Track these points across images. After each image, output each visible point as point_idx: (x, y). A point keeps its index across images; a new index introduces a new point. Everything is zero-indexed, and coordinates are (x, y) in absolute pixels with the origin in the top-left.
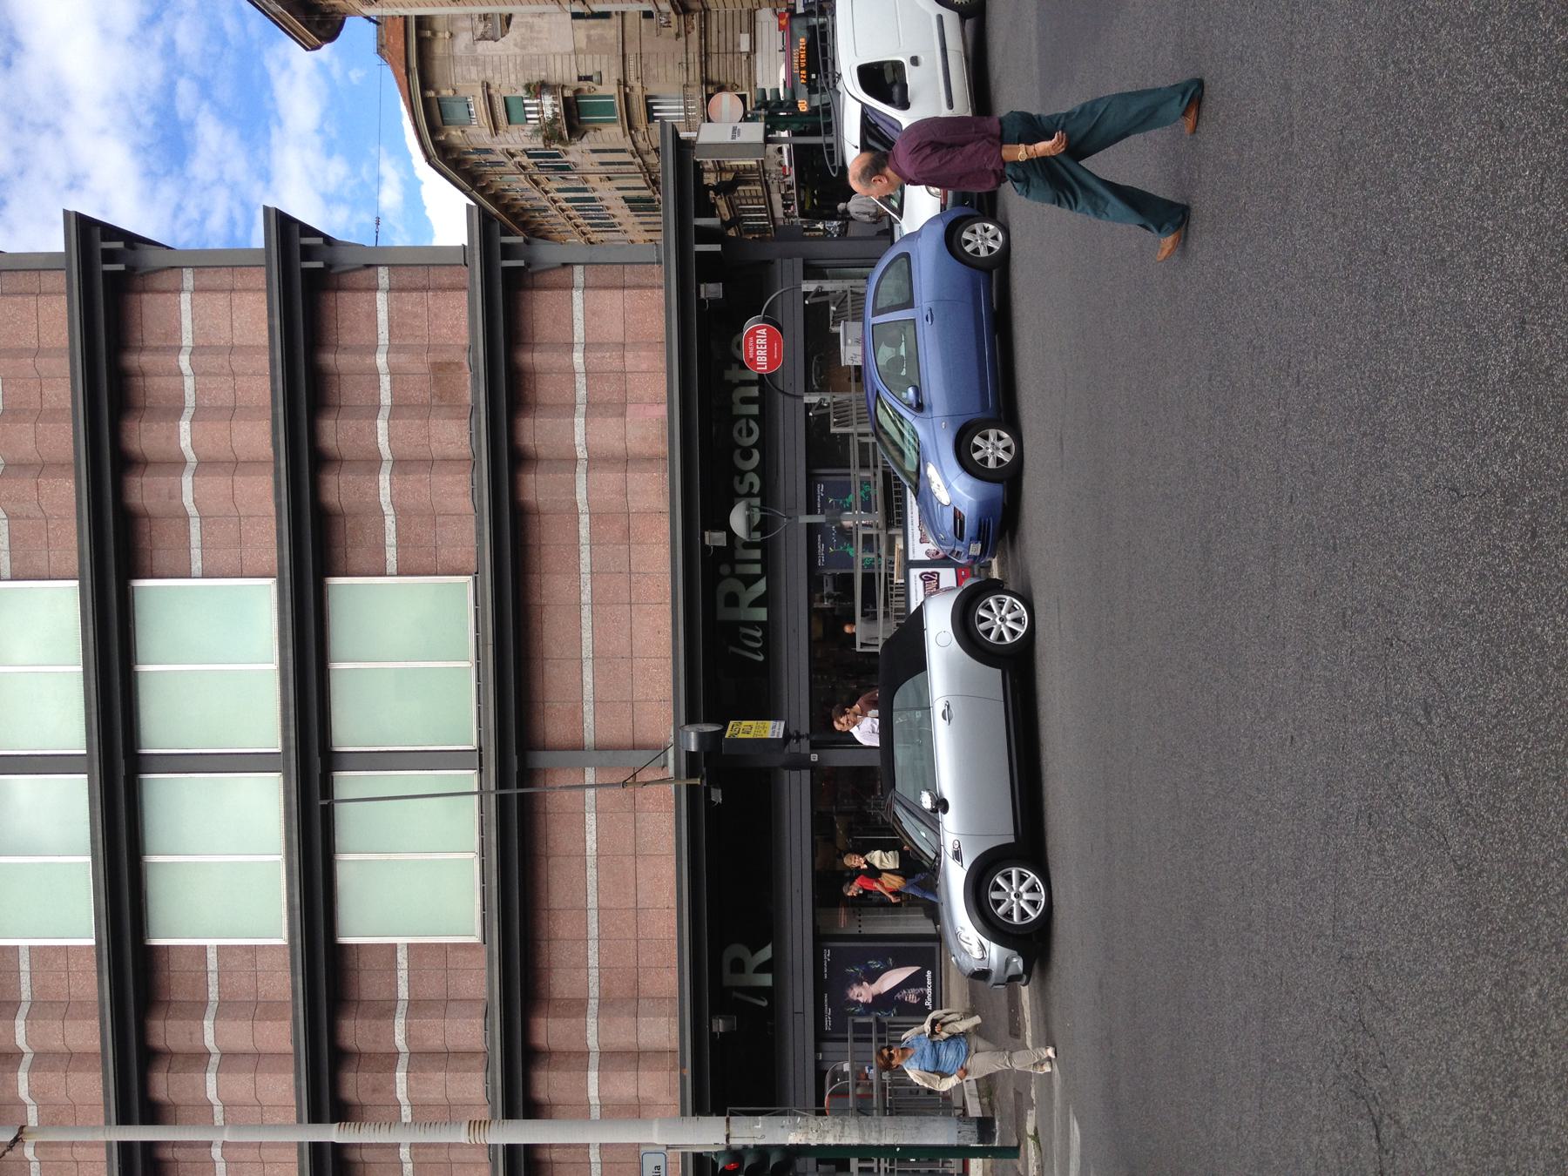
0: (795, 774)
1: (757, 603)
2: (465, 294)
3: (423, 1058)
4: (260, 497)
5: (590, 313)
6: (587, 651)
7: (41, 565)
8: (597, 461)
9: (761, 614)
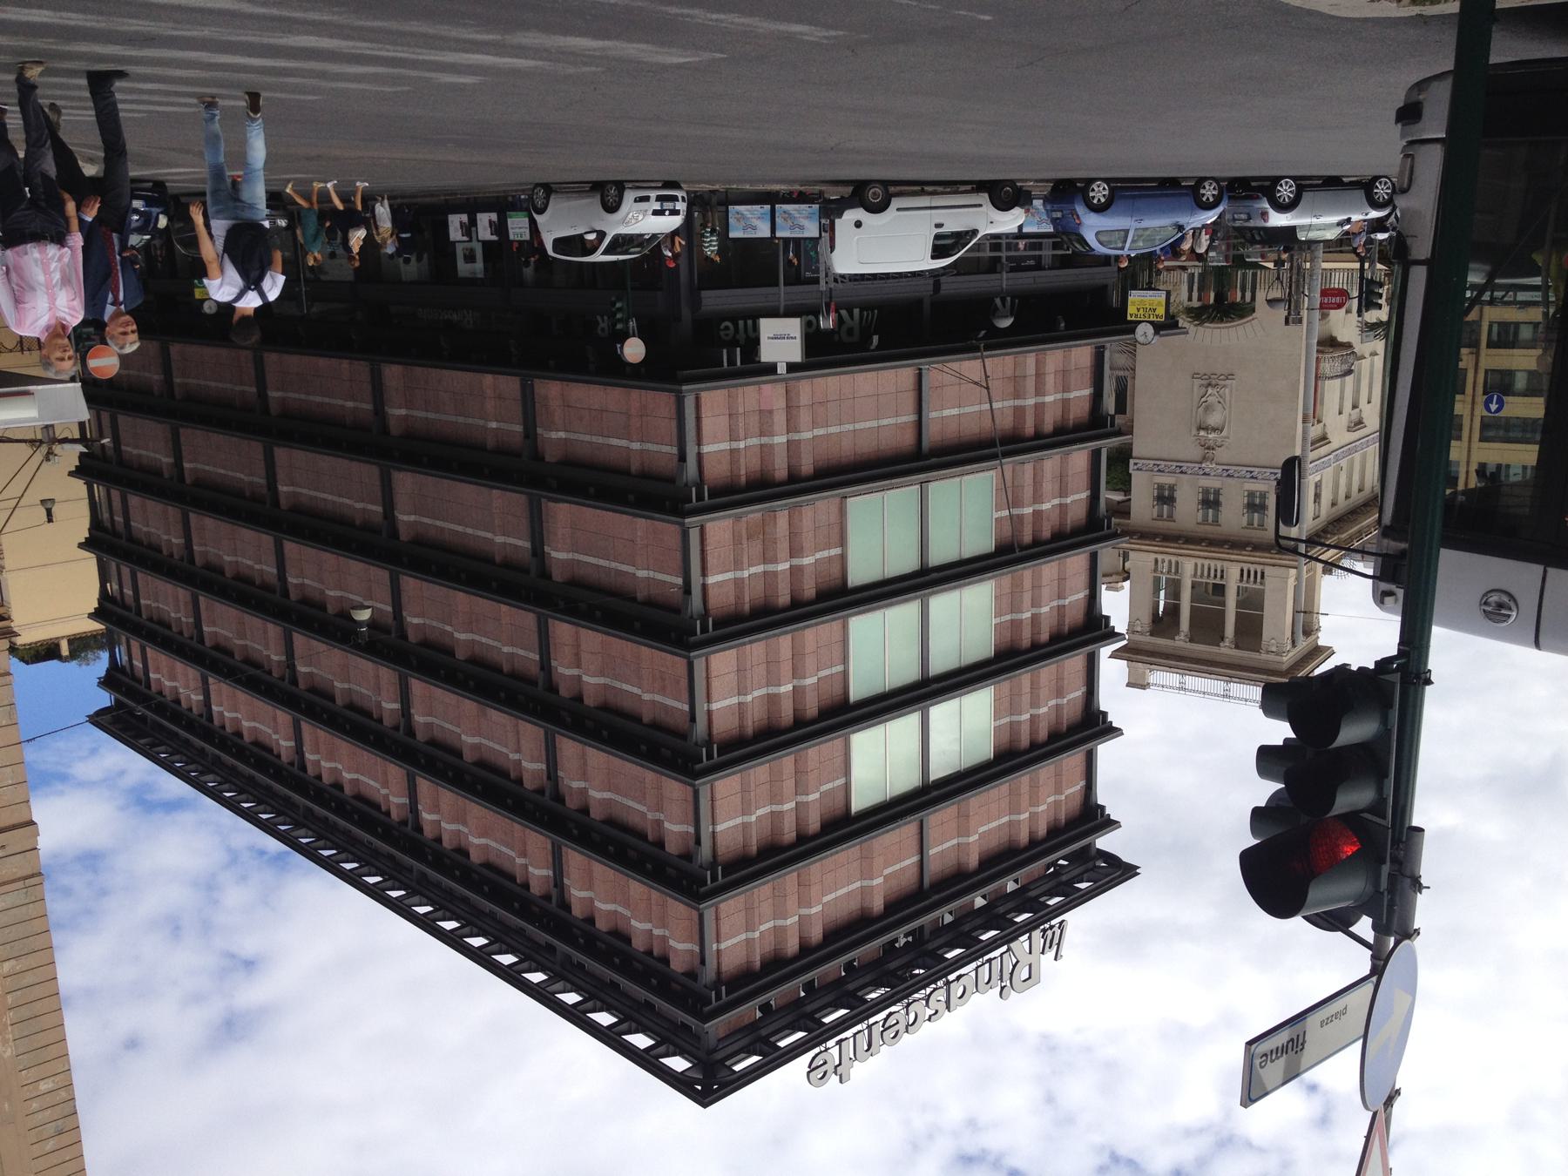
0: (943, 287)
1: (851, 315)
2: (709, 526)
3: (1037, 498)
4: (816, 634)
5: (715, 441)
6: (874, 424)
7: (839, 760)
8: (791, 427)
9: (856, 311)
